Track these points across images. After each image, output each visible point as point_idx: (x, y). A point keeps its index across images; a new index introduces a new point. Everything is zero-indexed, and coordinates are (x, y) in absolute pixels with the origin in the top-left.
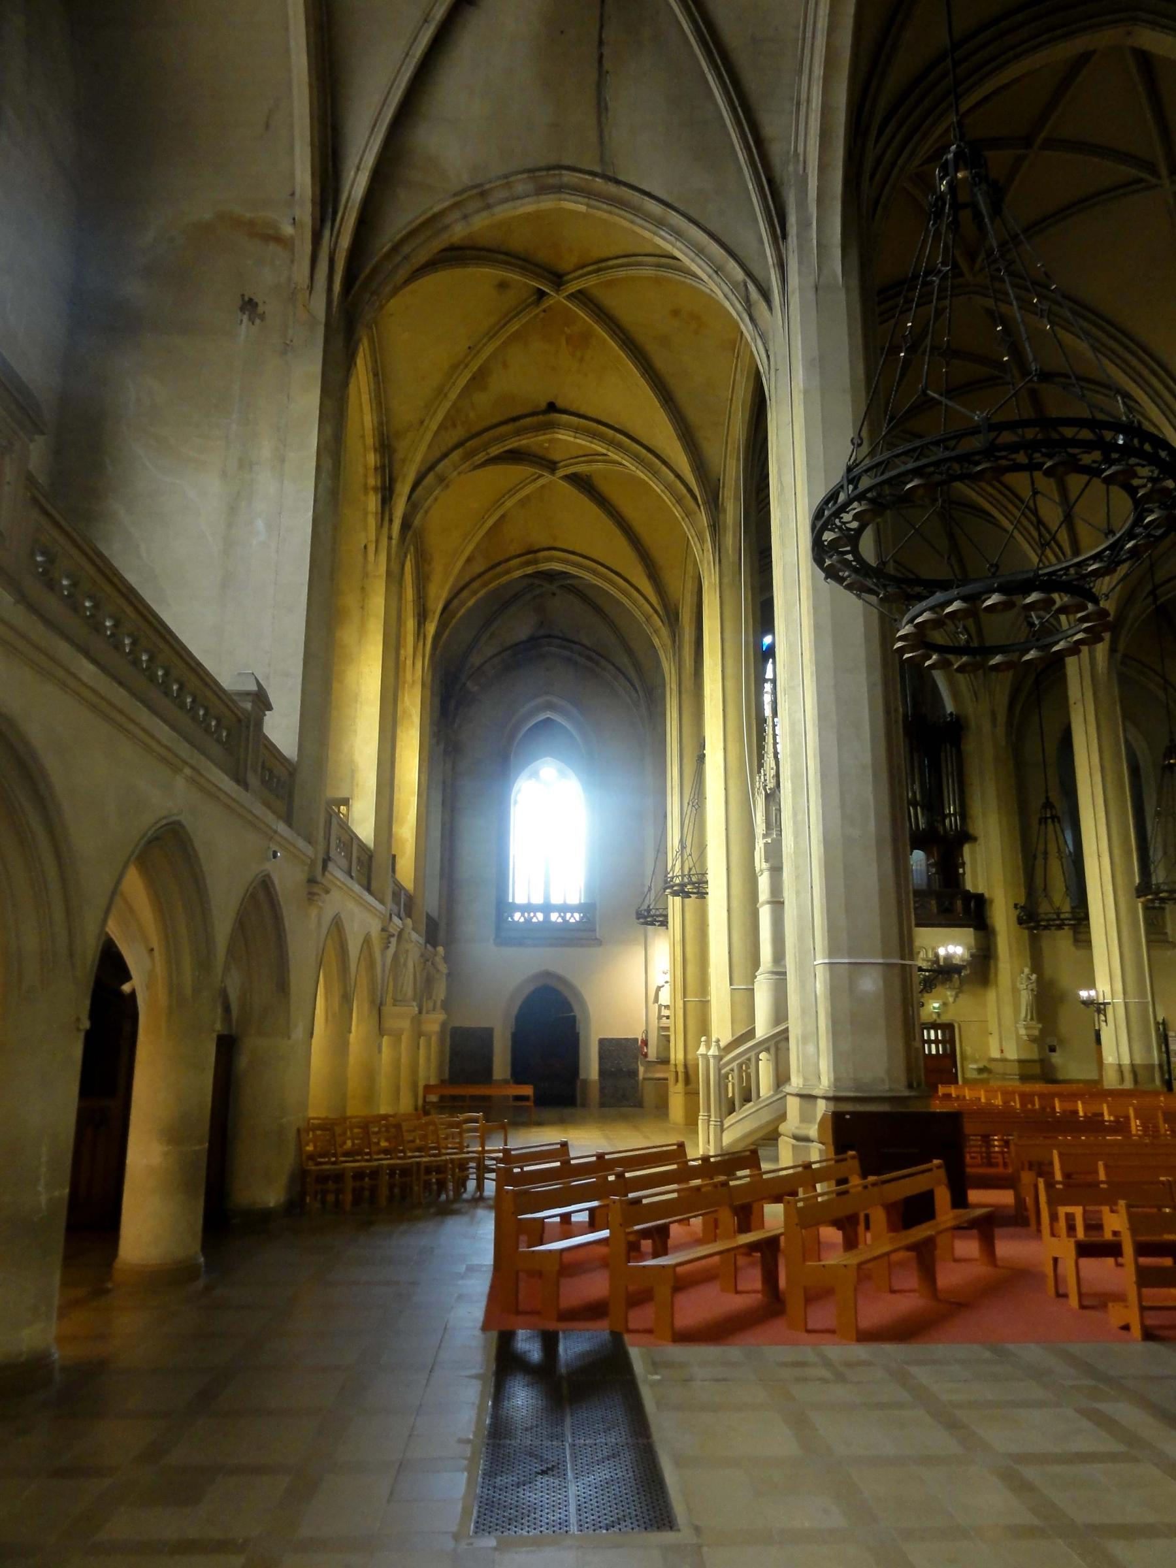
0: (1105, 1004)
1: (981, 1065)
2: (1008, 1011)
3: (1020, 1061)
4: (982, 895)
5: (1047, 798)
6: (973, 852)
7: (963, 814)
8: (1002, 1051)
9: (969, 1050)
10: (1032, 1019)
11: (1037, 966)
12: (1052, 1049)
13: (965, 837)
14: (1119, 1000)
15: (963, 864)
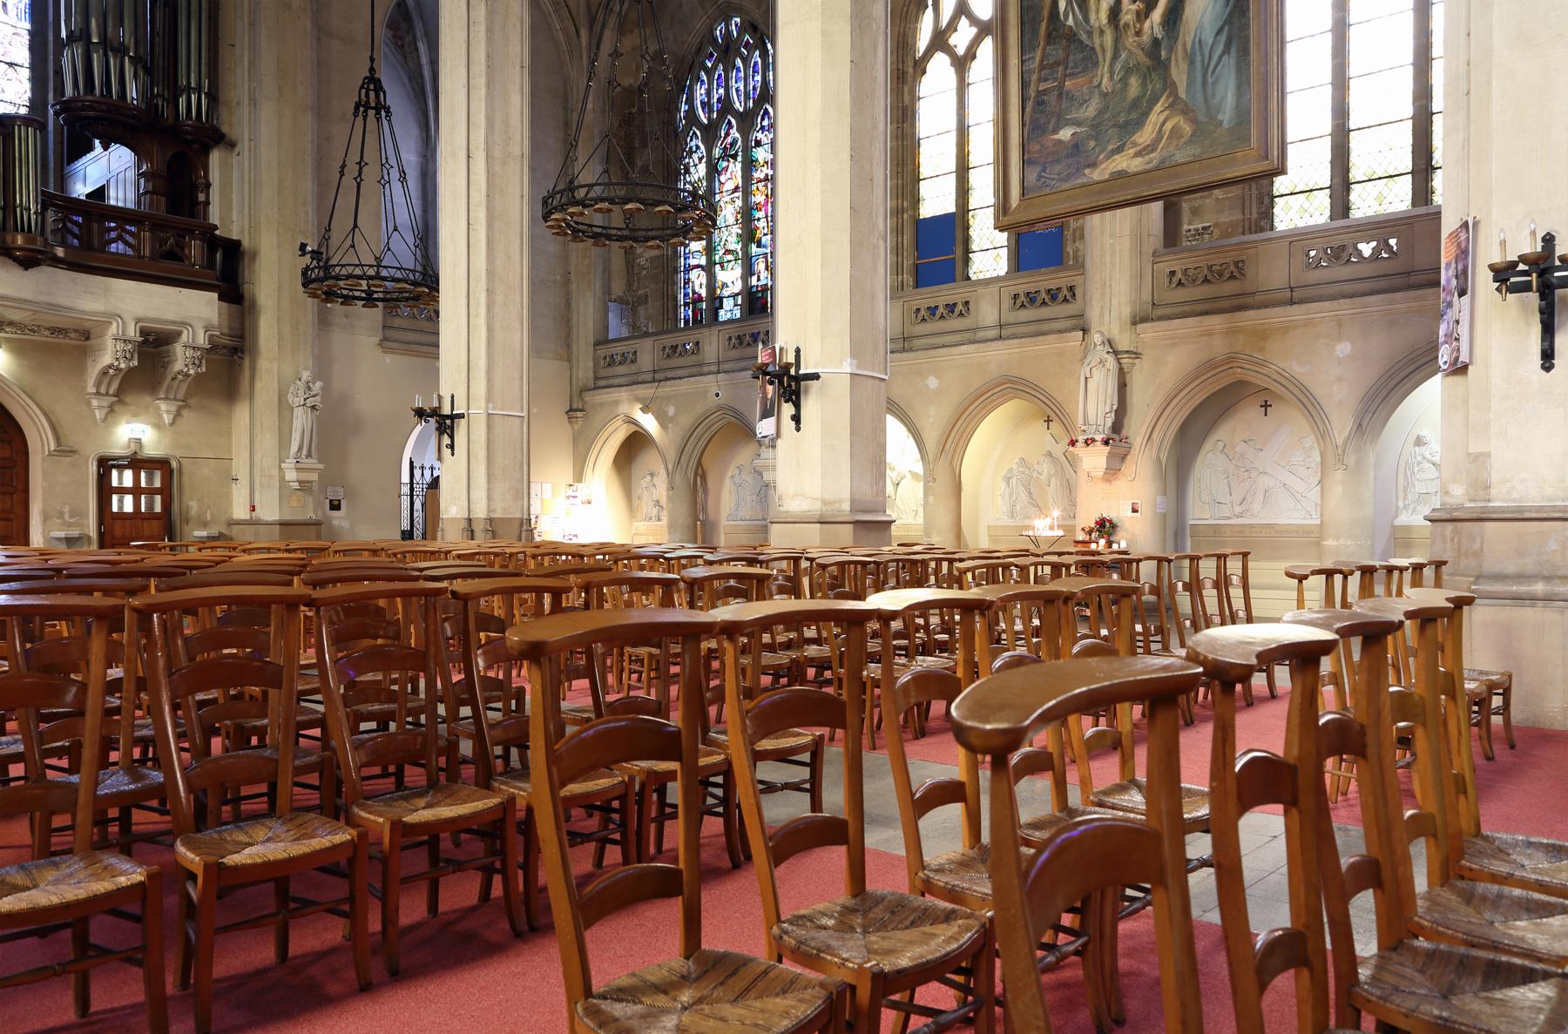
0: (453, 417)
1: (214, 531)
2: (267, 441)
3: (283, 524)
4: (238, 243)
5: (372, 70)
6: (226, 167)
7: (213, 98)
8: (253, 509)
9: (194, 507)
10: (309, 455)
11: (323, 368)
12: (335, 506)
13: (213, 137)
14: (478, 410)
15: (208, 185)
